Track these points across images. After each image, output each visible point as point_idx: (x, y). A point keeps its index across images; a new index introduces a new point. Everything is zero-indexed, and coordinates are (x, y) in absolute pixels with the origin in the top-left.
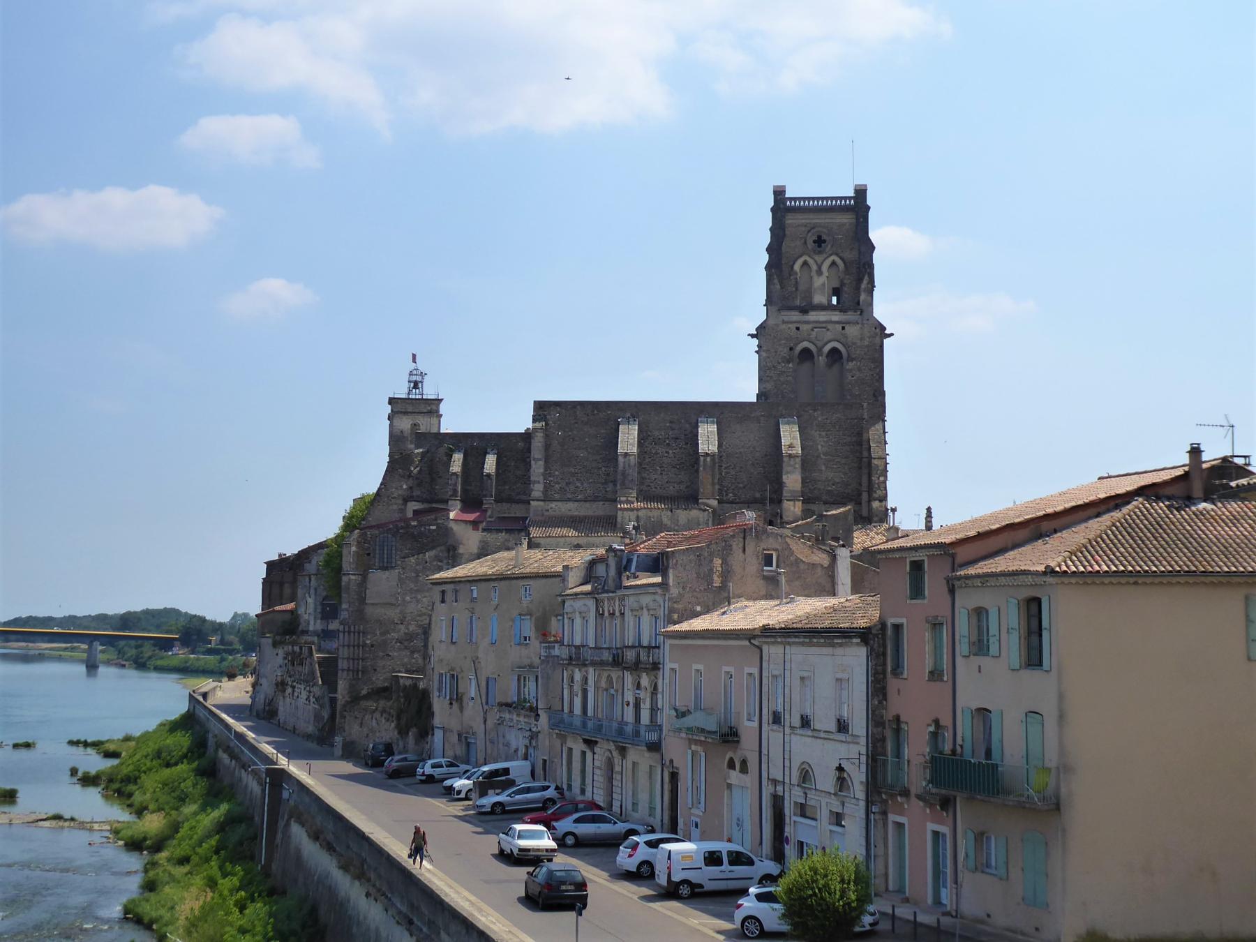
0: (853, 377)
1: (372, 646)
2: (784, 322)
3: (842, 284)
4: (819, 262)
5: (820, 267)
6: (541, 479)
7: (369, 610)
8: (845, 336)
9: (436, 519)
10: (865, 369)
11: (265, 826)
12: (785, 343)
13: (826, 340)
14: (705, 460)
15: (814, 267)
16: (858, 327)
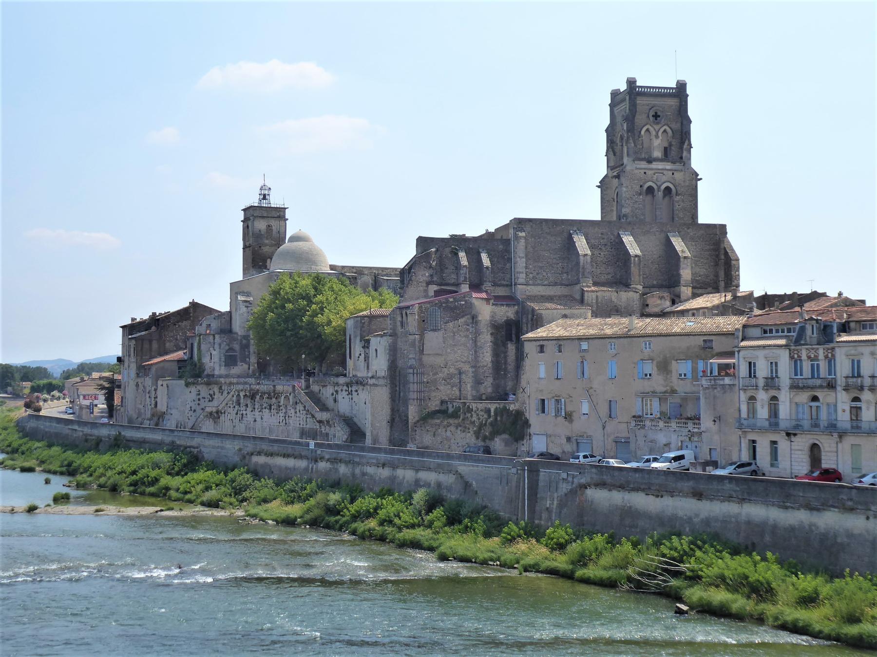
1: (428, 383)
2: (637, 169)
3: (670, 145)
5: (657, 133)
6: (524, 270)
7: (425, 359)
8: (673, 178)
9: (464, 297)
11: (526, 495)
13: (663, 181)
14: (634, 260)
15: (654, 133)
16: (682, 173)
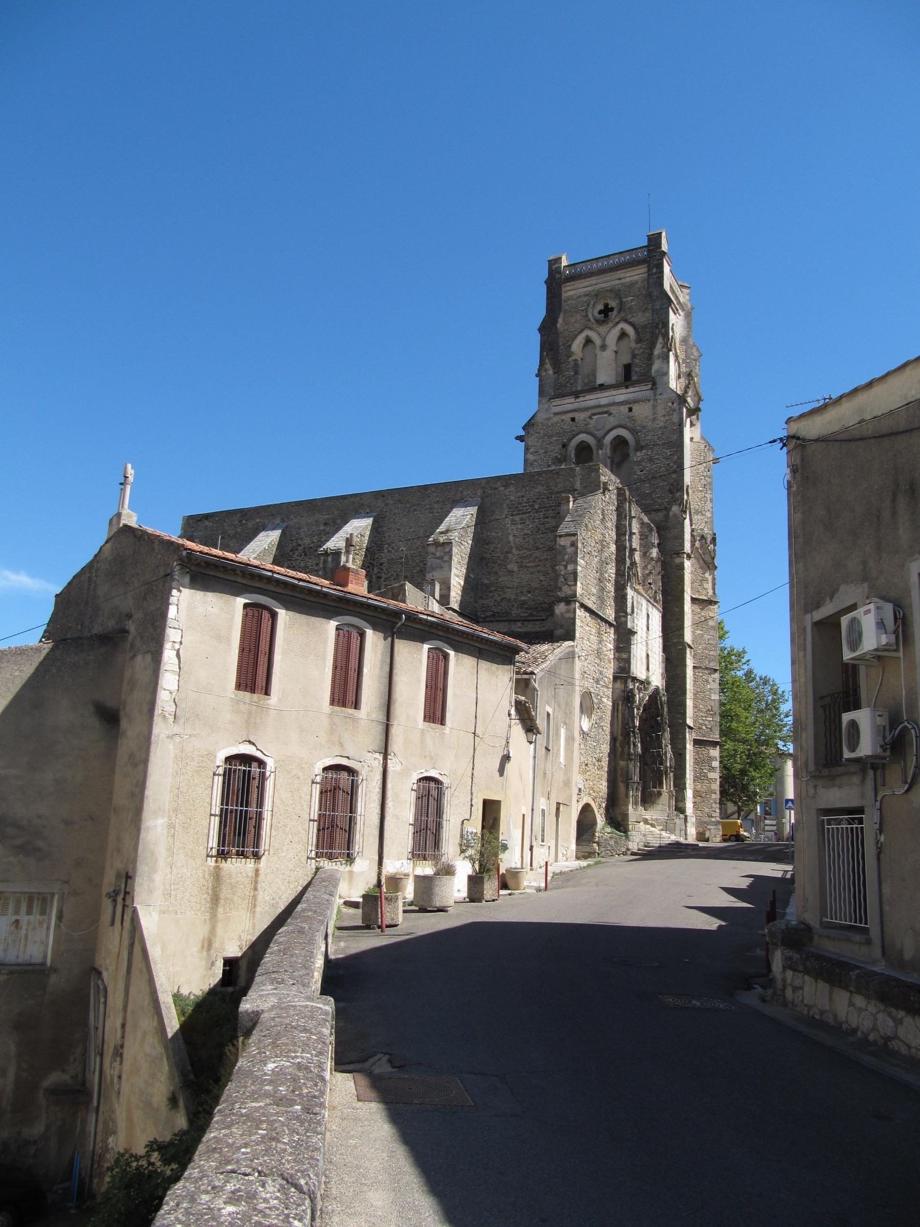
0: (642, 471)
3: (634, 356)
4: (603, 334)
10: (657, 459)
12: (557, 440)
13: (607, 428)
14: (325, 562)
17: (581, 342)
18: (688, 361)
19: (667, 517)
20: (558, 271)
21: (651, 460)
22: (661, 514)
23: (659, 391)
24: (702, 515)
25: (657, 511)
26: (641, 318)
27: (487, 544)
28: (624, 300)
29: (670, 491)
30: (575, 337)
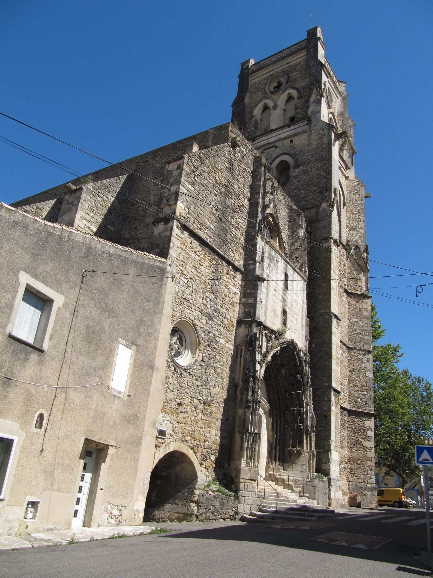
8: (293, 147)
10: (311, 171)
13: (274, 157)
16: (305, 136)
17: (260, 108)
18: (344, 127)
19: (317, 212)
20: (247, 68)
21: (306, 173)
22: (313, 211)
23: (313, 124)
24: (357, 231)
25: (309, 209)
26: (302, 84)
27: (132, 205)
28: (291, 75)
29: (321, 193)
30: (256, 106)
